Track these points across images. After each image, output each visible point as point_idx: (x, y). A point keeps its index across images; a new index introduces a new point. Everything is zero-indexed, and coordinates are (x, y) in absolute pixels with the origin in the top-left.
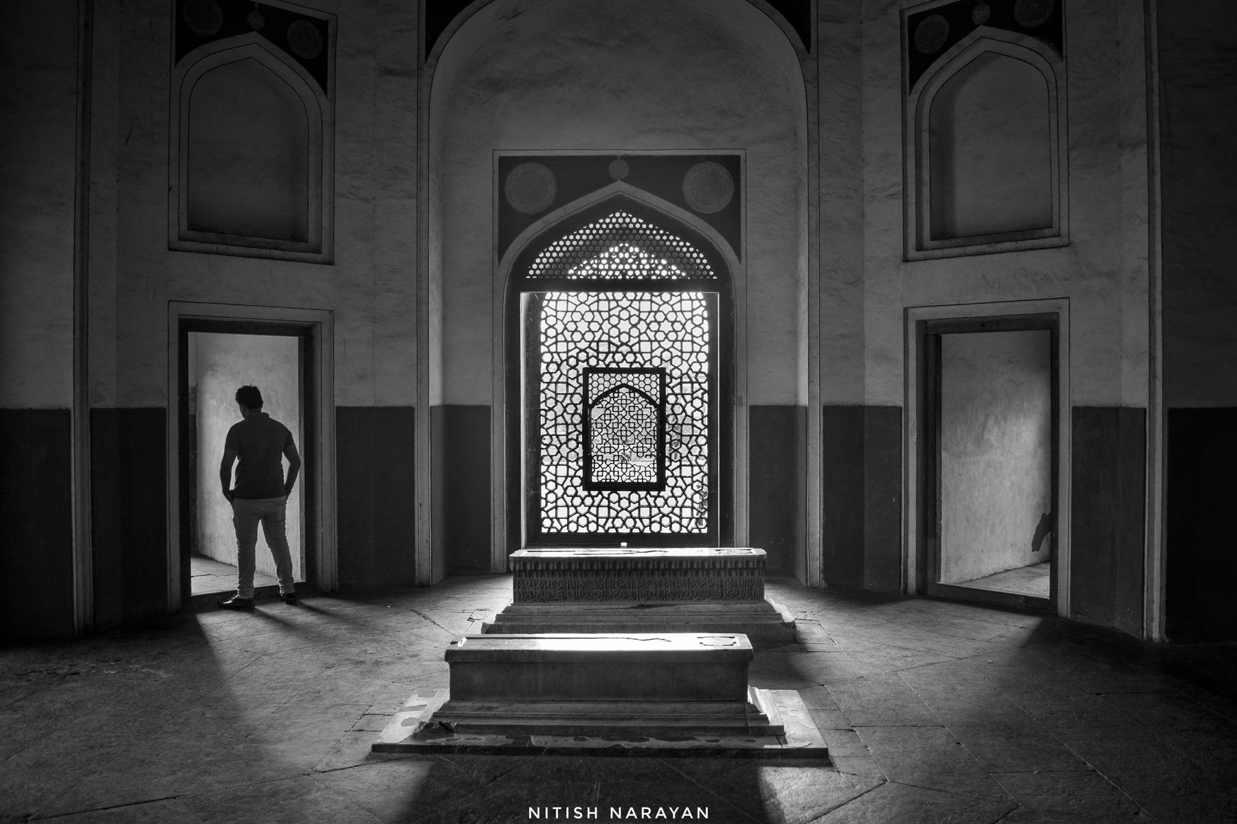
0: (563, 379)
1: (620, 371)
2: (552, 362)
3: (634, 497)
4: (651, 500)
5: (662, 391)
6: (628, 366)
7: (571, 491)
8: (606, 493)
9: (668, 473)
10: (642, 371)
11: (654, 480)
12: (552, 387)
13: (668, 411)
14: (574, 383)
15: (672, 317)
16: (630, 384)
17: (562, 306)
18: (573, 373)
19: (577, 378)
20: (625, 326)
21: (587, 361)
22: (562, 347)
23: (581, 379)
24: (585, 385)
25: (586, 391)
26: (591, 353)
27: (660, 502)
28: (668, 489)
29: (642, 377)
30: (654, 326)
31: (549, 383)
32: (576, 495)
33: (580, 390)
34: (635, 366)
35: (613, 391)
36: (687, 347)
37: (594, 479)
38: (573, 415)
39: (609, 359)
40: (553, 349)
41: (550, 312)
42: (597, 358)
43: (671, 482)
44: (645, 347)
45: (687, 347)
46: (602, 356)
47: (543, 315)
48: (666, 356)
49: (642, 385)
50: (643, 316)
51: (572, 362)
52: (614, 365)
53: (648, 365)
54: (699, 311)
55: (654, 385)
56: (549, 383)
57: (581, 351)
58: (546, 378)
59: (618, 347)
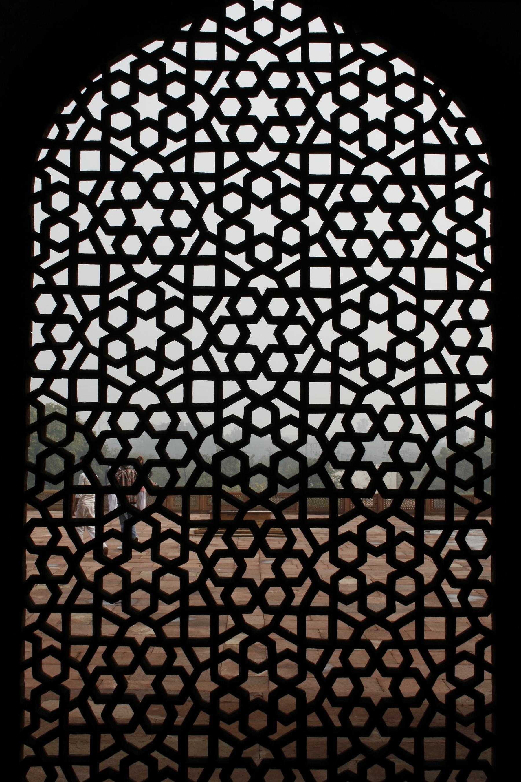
0: (92, 362)
2: (59, 316)
12: (60, 386)
15: (394, 194)
17: (90, 161)
20: (263, 220)
22: (89, 275)
30: (346, 221)
31: (49, 376)
36: (436, 279)
40: (61, 278)
41: (56, 176)
45: (436, 279)
47: (38, 185)
50: (315, 190)
54: (469, 181)
56: (49, 376)
58: (45, 360)
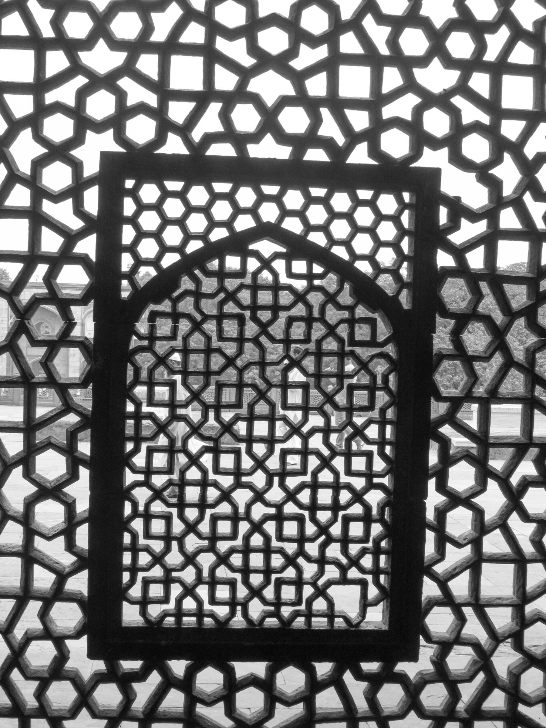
1: (245, 171)
3: (291, 679)
4: (357, 689)
5: (422, 260)
6: (284, 153)
7: (40, 654)
8: (178, 667)
9: (430, 589)
10: (338, 175)
11: (376, 617)
13: (441, 341)
14: (62, 212)
16: (293, 225)
18: (57, 176)
19: (75, 192)
21: (116, 122)
23: (92, 200)
24: (106, 225)
25: (110, 248)
26: (137, 93)
27: (391, 696)
28: (427, 652)
29: (341, 201)
32: (58, 670)
33: (88, 246)
34: (316, 155)
35: (218, 250)
37: (131, 615)
38: (53, 347)
39: (210, 121)
42: (159, 114)
43: (439, 621)
44: (355, 82)
46: (179, 111)
48: (436, 123)
49: (341, 229)
51: (59, 128)
52: (223, 150)
53: (360, 155)
55: (387, 231)
57: (96, 82)
59: (245, 74)
